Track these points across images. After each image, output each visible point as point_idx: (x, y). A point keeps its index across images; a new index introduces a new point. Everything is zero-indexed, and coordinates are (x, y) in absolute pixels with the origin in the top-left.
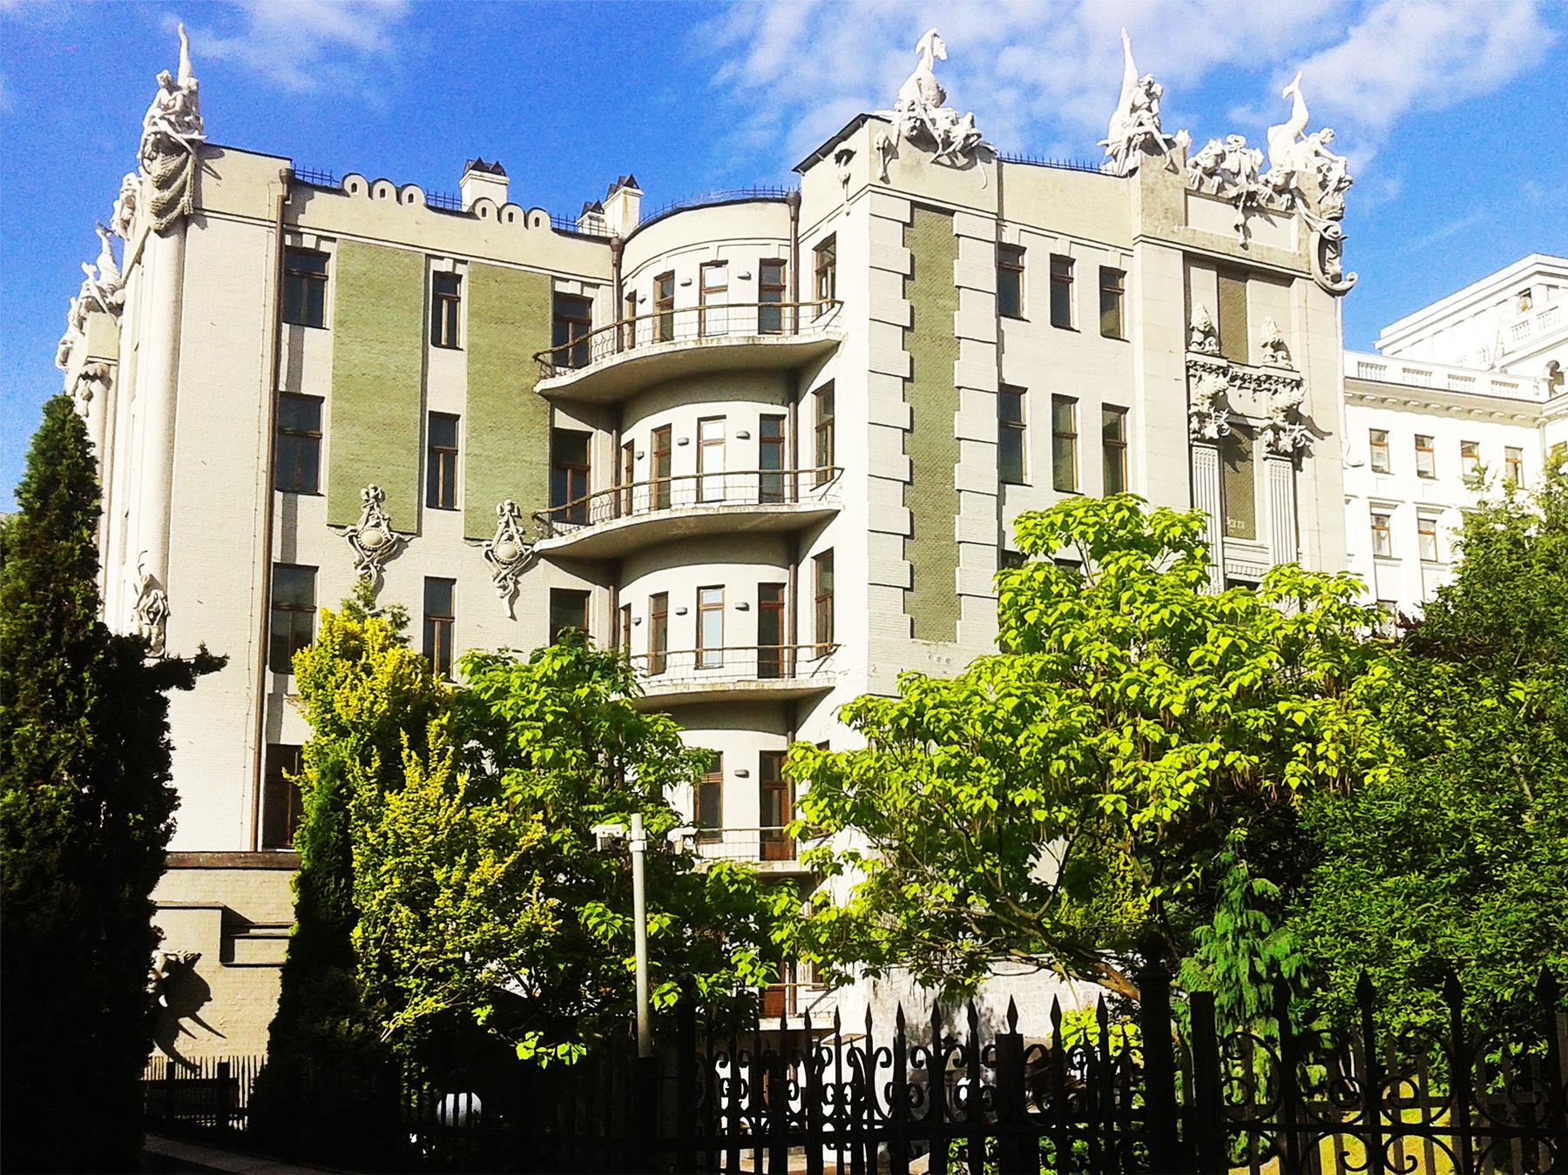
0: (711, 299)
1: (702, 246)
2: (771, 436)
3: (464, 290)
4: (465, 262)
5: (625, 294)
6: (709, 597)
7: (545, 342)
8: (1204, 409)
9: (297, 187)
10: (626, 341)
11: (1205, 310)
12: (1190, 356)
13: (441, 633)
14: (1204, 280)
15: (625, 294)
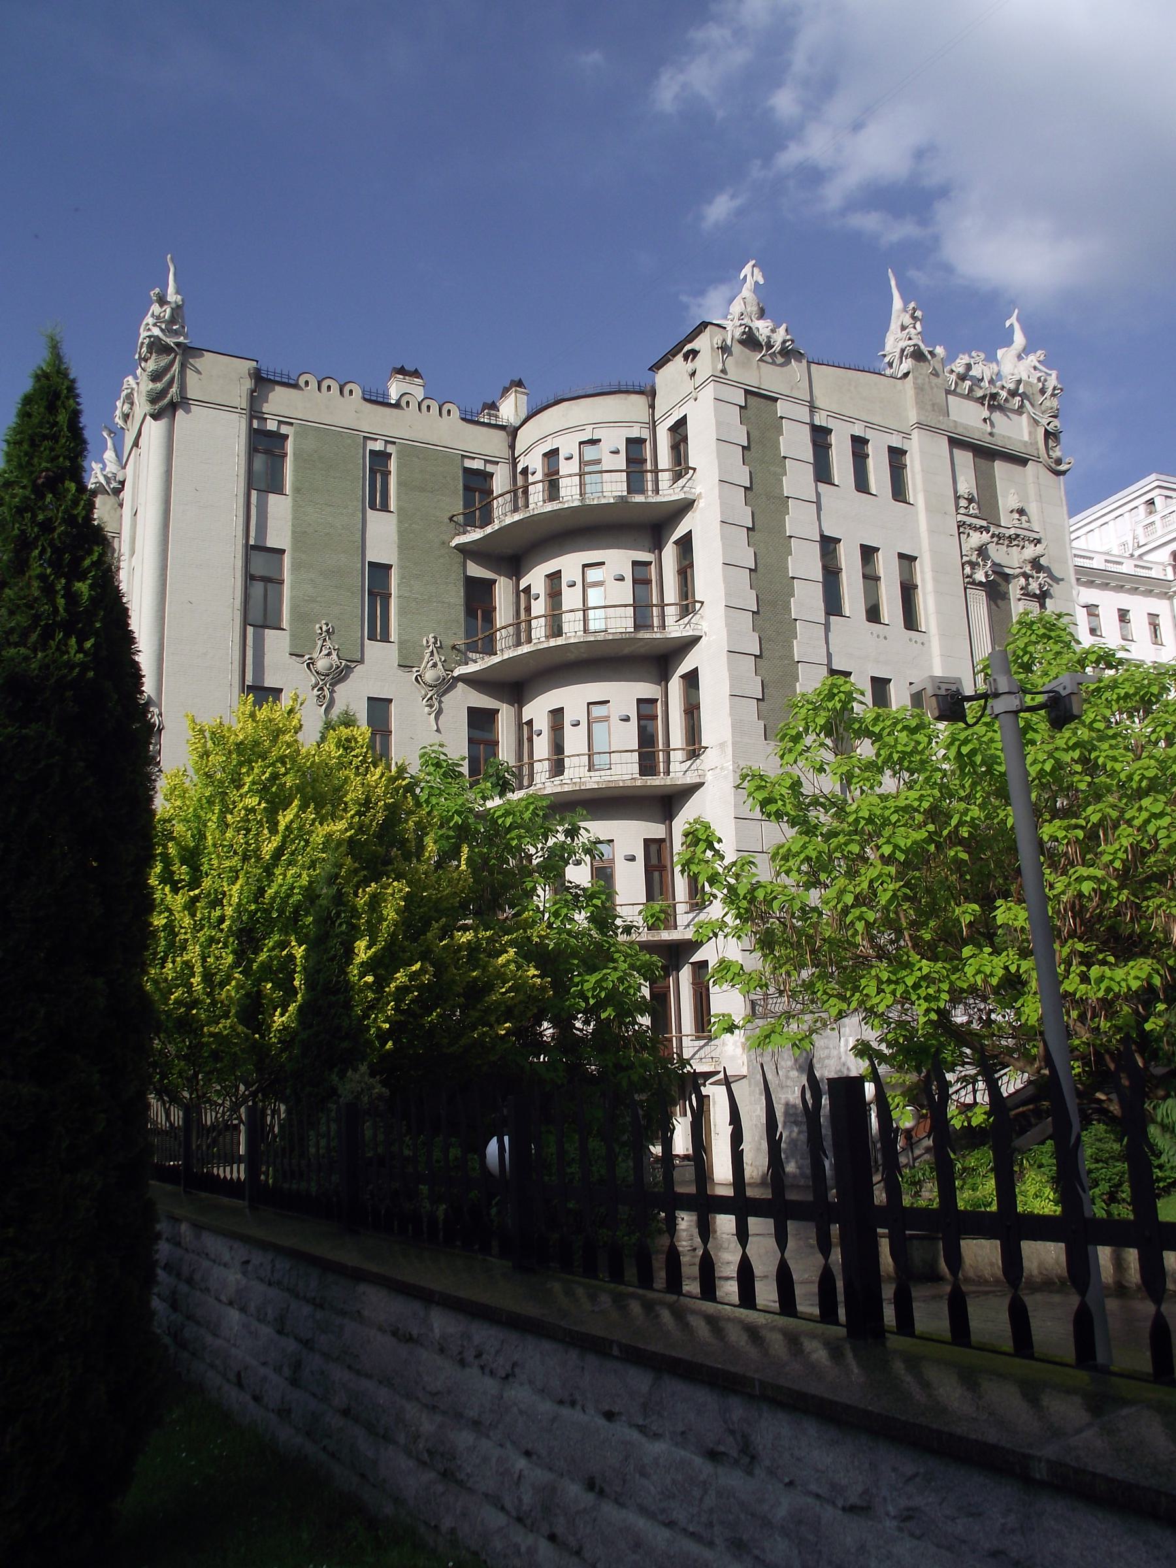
0: (587, 469)
1: (580, 428)
2: (641, 578)
3: (393, 465)
4: (394, 443)
5: (519, 468)
6: (597, 711)
7: (459, 507)
8: (974, 558)
9: (262, 382)
10: (521, 503)
11: (967, 484)
12: (960, 518)
13: (381, 744)
14: (965, 458)
15: (519, 468)
